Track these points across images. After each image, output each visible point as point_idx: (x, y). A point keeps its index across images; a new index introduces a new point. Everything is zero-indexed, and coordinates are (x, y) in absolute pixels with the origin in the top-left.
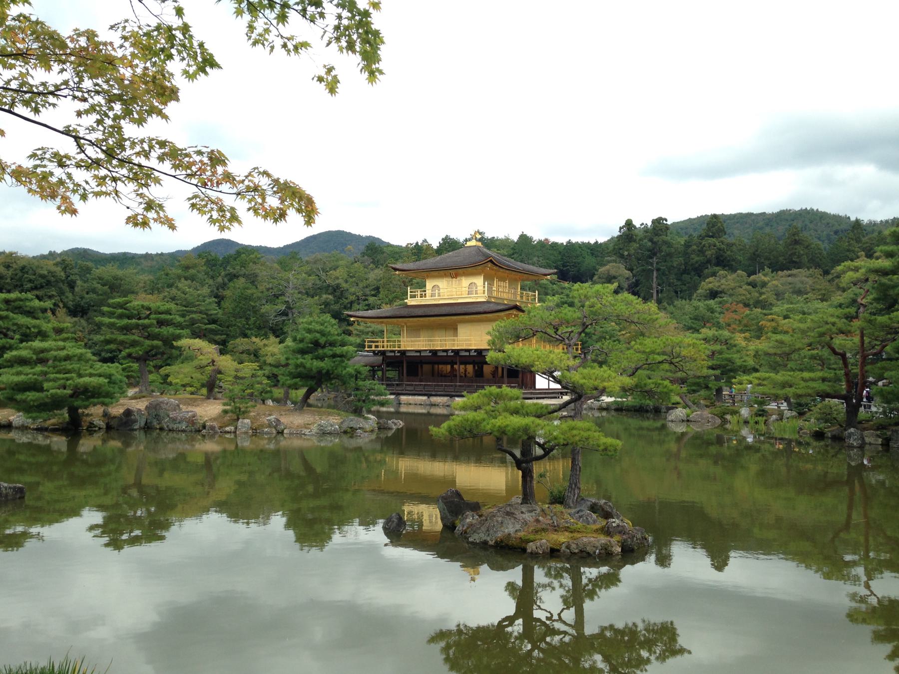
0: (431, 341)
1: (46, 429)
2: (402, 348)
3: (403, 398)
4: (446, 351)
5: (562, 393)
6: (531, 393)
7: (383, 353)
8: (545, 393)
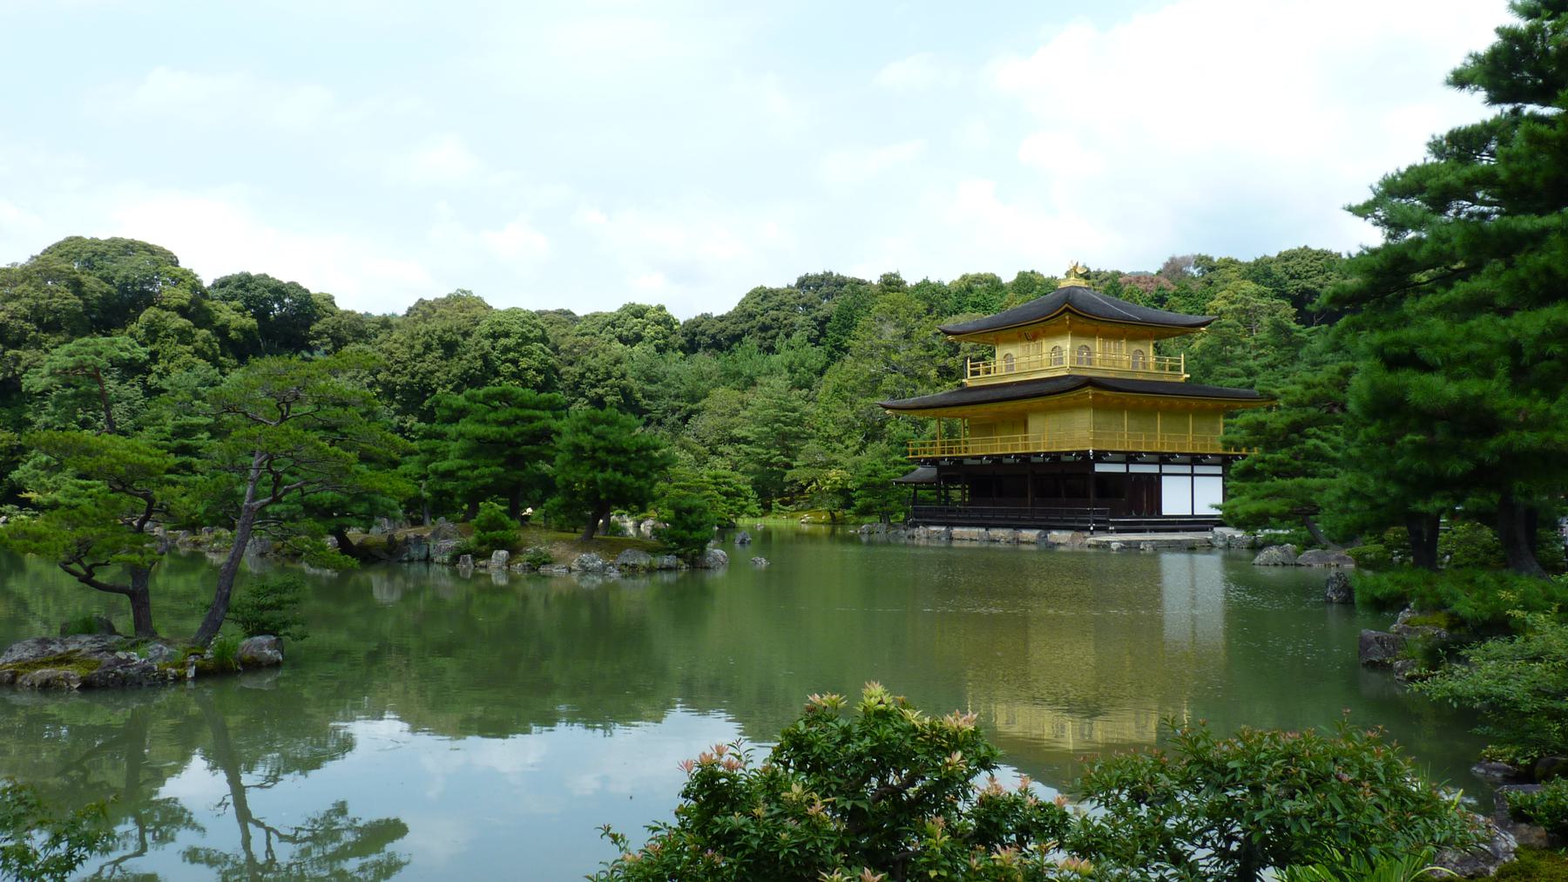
3: (956, 530)
4: (1008, 456)
5: (1221, 524)
7: (934, 462)
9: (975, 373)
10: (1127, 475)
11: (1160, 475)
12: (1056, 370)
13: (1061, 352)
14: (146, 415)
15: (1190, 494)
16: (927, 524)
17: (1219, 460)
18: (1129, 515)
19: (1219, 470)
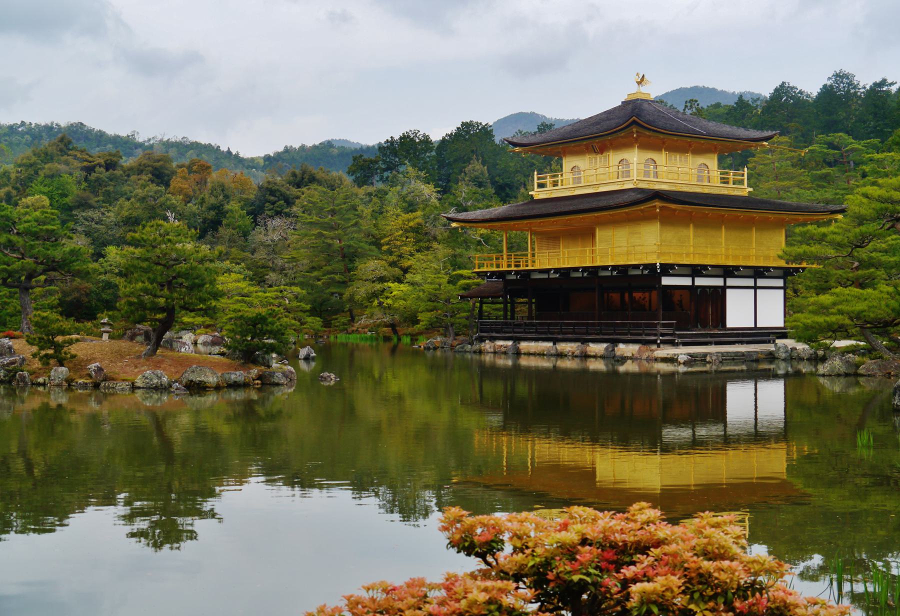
2: (521, 268)
3: (524, 345)
4: (576, 269)
5: (784, 336)
7: (501, 275)
8: (738, 335)
9: (541, 186)
10: (693, 288)
11: (724, 288)
13: (628, 165)
14: (437, 223)
15: (753, 308)
16: (493, 339)
17: (780, 273)
18: (695, 327)
19: (780, 282)
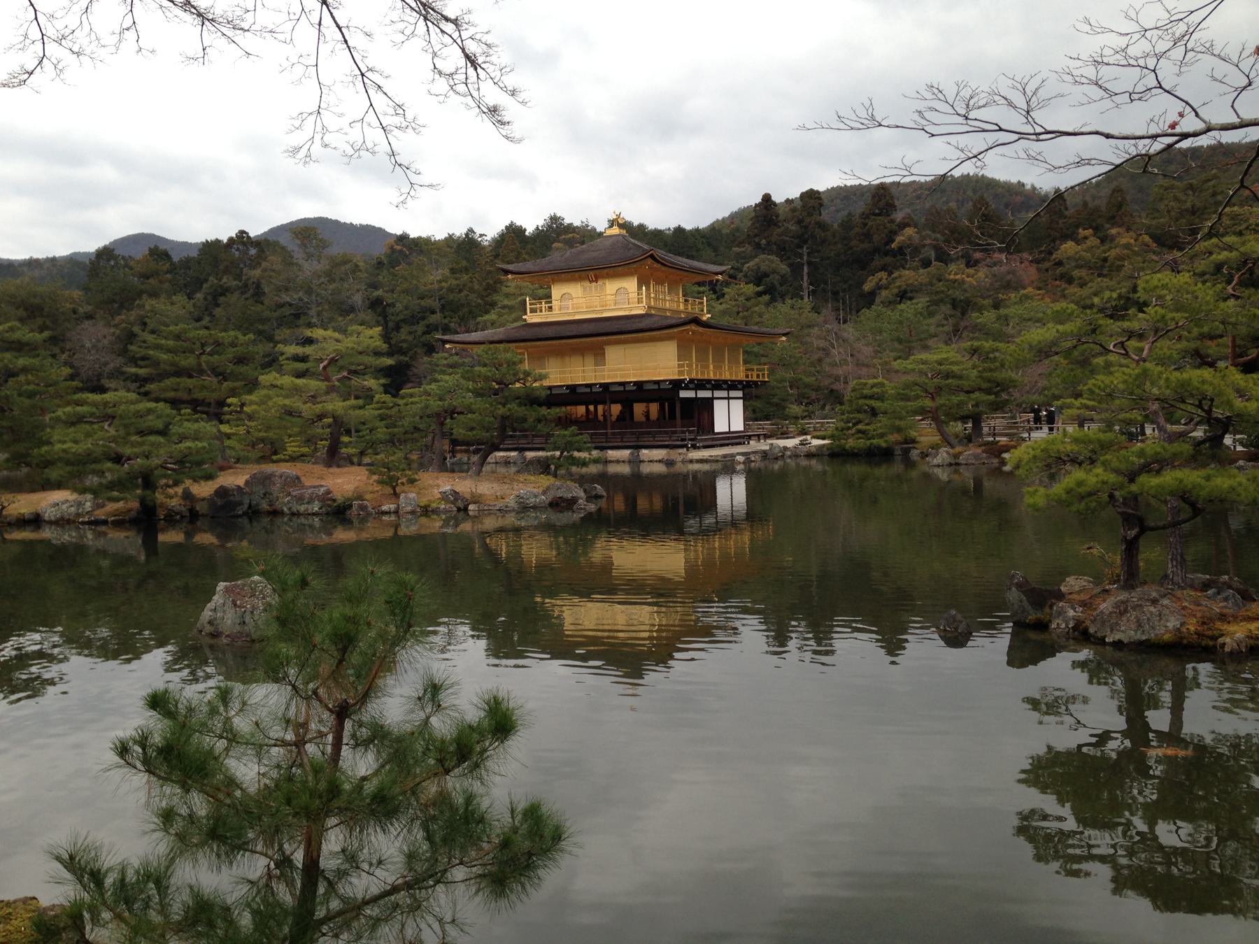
0: (564, 372)
1: (105, 522)
6: (713, 439)
8: (728, 438)
11: (713, 399)
12: (631, 309)
15: (729, 415)
19: (740, 394)
